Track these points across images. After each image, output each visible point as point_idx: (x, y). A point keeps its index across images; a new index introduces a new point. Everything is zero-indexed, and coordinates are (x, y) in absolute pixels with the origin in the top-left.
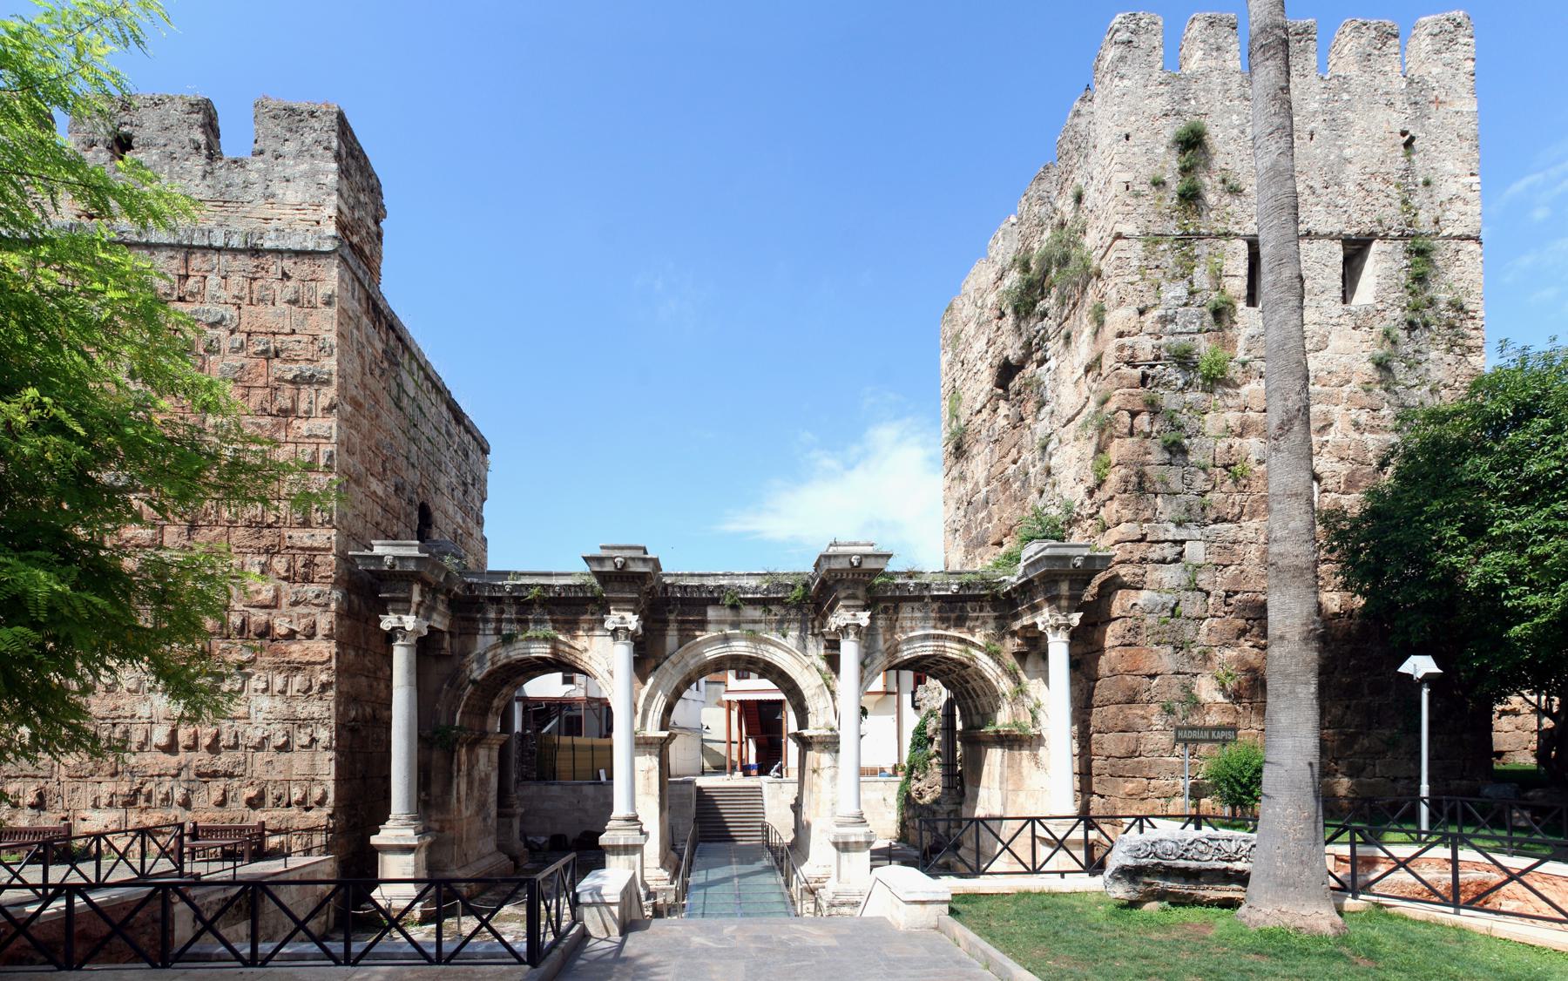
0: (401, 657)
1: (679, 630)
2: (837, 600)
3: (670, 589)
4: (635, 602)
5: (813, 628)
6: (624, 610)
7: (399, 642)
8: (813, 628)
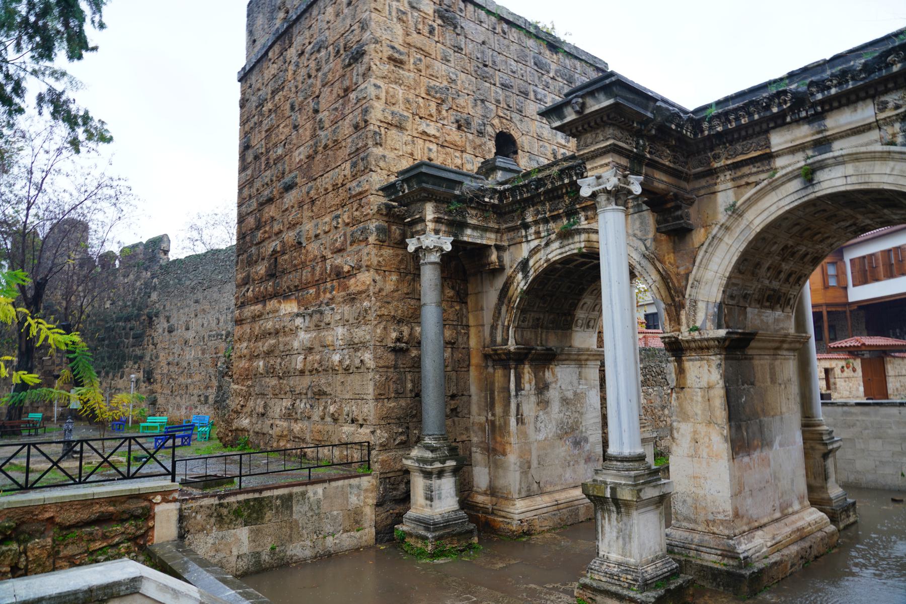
0: (429, 276)
1: (733, 180)
3: (705, 125)
4: (614, 150)
6: (601, 166)
7: (422, 261)
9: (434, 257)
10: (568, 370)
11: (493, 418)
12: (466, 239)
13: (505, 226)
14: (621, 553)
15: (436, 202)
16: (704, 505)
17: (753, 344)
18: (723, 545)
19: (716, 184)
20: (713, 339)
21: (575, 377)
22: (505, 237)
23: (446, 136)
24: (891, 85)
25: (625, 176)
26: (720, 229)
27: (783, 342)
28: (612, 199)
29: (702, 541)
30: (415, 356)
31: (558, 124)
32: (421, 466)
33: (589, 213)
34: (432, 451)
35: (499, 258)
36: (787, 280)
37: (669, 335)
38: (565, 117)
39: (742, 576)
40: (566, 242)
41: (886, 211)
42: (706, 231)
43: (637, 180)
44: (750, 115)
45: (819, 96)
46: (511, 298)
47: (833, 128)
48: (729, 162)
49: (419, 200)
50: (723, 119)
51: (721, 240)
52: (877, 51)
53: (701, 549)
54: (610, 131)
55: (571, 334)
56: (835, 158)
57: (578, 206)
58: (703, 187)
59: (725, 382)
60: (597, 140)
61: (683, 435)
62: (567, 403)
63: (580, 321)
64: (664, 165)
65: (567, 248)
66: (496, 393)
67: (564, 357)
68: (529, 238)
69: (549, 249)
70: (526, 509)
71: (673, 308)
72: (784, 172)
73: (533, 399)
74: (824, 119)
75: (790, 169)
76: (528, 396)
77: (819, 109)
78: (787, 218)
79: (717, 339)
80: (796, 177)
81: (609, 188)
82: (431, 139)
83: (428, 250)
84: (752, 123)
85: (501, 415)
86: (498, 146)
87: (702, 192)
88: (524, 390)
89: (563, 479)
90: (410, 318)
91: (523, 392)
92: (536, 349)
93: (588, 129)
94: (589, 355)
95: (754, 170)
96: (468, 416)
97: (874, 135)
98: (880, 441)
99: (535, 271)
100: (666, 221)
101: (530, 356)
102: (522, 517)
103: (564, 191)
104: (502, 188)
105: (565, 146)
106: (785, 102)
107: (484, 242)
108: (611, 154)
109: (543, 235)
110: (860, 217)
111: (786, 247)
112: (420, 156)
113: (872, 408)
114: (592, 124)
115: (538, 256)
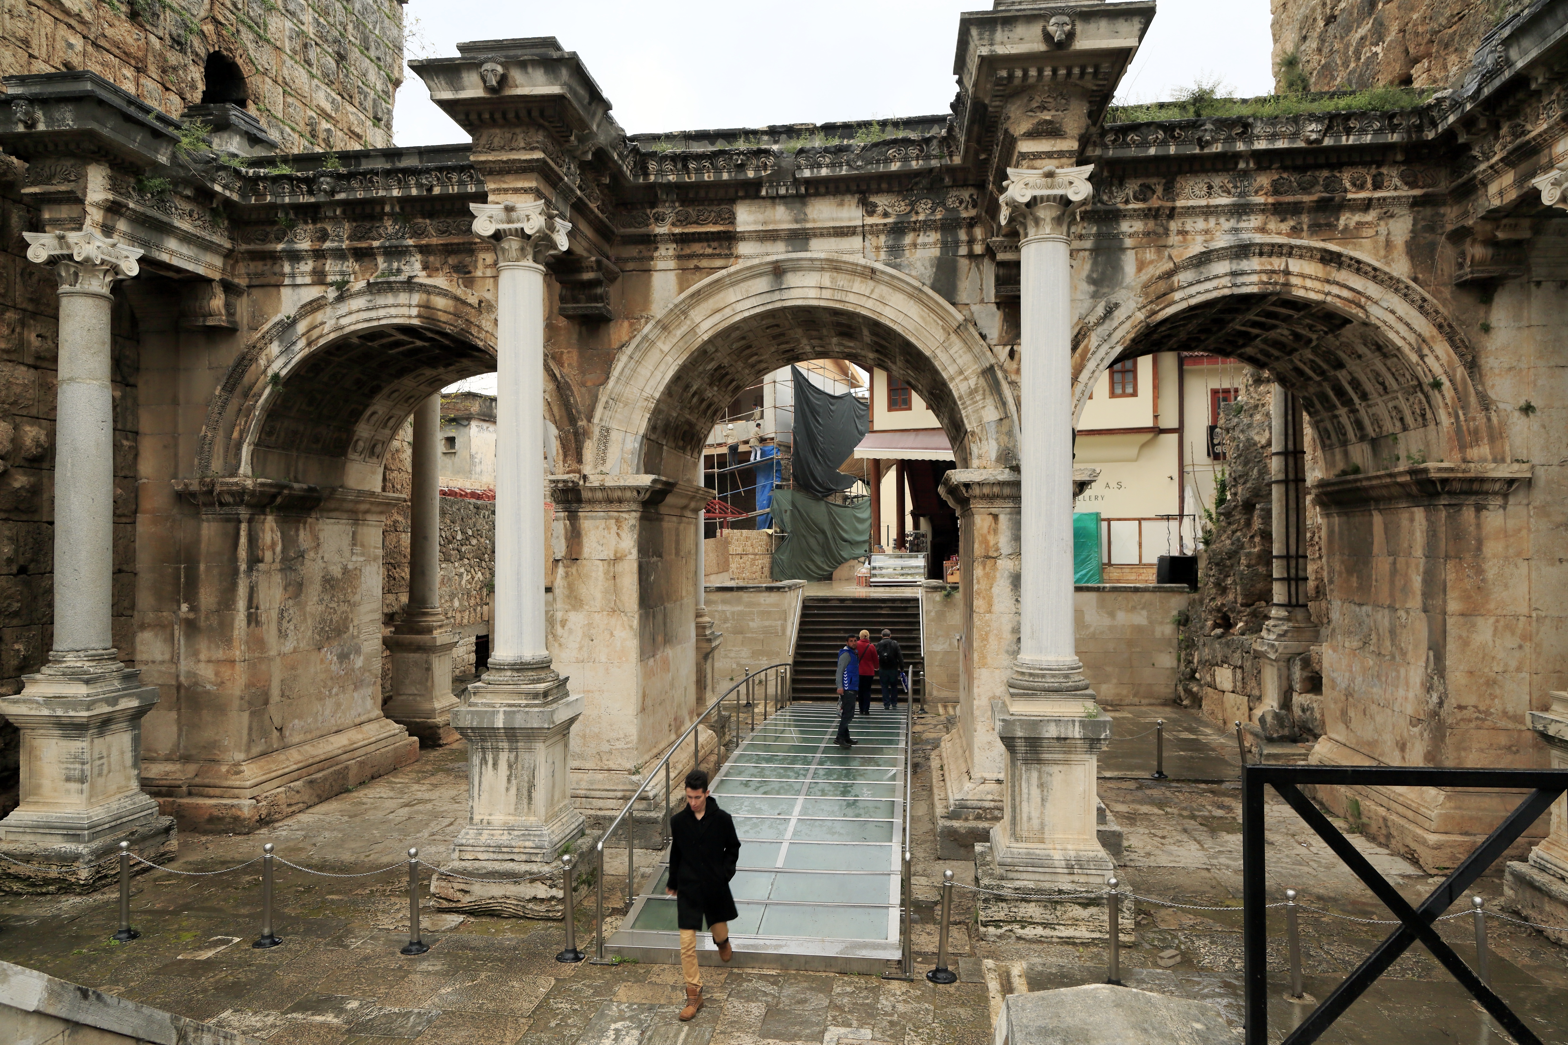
1: (679, 257)
2: (1011, 141)
3: (652, 166)
4: (541, 169)
5: (971, 242)
6: (516, 191)
8: (971, 242)
9: (100, 285)
10: (336, 528)
11: (191, 616)
12: (165, 257)
13: (244, 247)
14: (512, 811)
15: (111, 167)
16: (597, 730)
17: (670, 499)
18: (624, 784)
19: (652, 258)
20: (630, 488)
21: (346, 541)
22: (241, 268)
23: (106, 26)
24: (884, 186)
25: (550, 217)
26: (655, 327)
27: (692, 498)
28: (530, 250)
29: (592, 782)
30: (22, 487)
31: (447, 95)
32: (59, 712)
33: (431, 259)
34: (87, 682)
35: (228, 305)
36: (705, 412)
37: (566, 477)
38: (463, 89)
39: (654, 821)
40: (381, 300)
41: (835, 340)
42: (631, 325)
43: (563, 226)
44: (718, 170)
45: (807, 173)
46: (250, 388)
47: (814, 221)
48: (677, 230)
49: (71, 155)
50: (680, 166)
51: (653, 343)
52: (875, 137)
53: (593, 793)
54: (539, 137)
55: (344, 464)
56: (812, 260)
57: (410, 242)
58: (633, 259)
59: (639, 551)
60: (514, 145)
61: (571, 631)
62: (332, 587)
63: (361, 444)
64: (592, 212)
65: (382, 313)
66: (202, 567)
67: (333, 504)
68: (299, 280)
69: (343, 308)
70: (264, 778)
71: (571, 437)
72: (749, 263)
73: (277, 578)
74: (804, 204)
75: (756, 261)
76: (268, 572)
77: (803, 190)
78: (738, 328)
79: (638, 490)
80: (761, 275)
81: (528, 231)
82: (73, 22)
83: (88, 264)
84: (718, 185)
85: (214, 607)
86: (208, 76)
87: (630, 266)
88: (261, 561)
89: (320, 719)
90: (11, 404)
91: (261, 566)
92: (291, 488)
93: (500, 121)
94: (372, 503)
95: (709, 251)
96: (129, 612)
97: (856, 242)
98: (740, 637)
99: (309, 344)
100: (575, 300)
101: (279, 500)
102: (255, 791)
103: (387, 209)
104: (251, 172)
105: (330, 116)
106: (765, 167)
107: (201, 270)
108: (535, 175)
109: (330, 279)
110: (804, 341)
111: (720, 367)
112: (44, 49)
113: (735, 594)
114: (511, 115)
115: (319, 316)
